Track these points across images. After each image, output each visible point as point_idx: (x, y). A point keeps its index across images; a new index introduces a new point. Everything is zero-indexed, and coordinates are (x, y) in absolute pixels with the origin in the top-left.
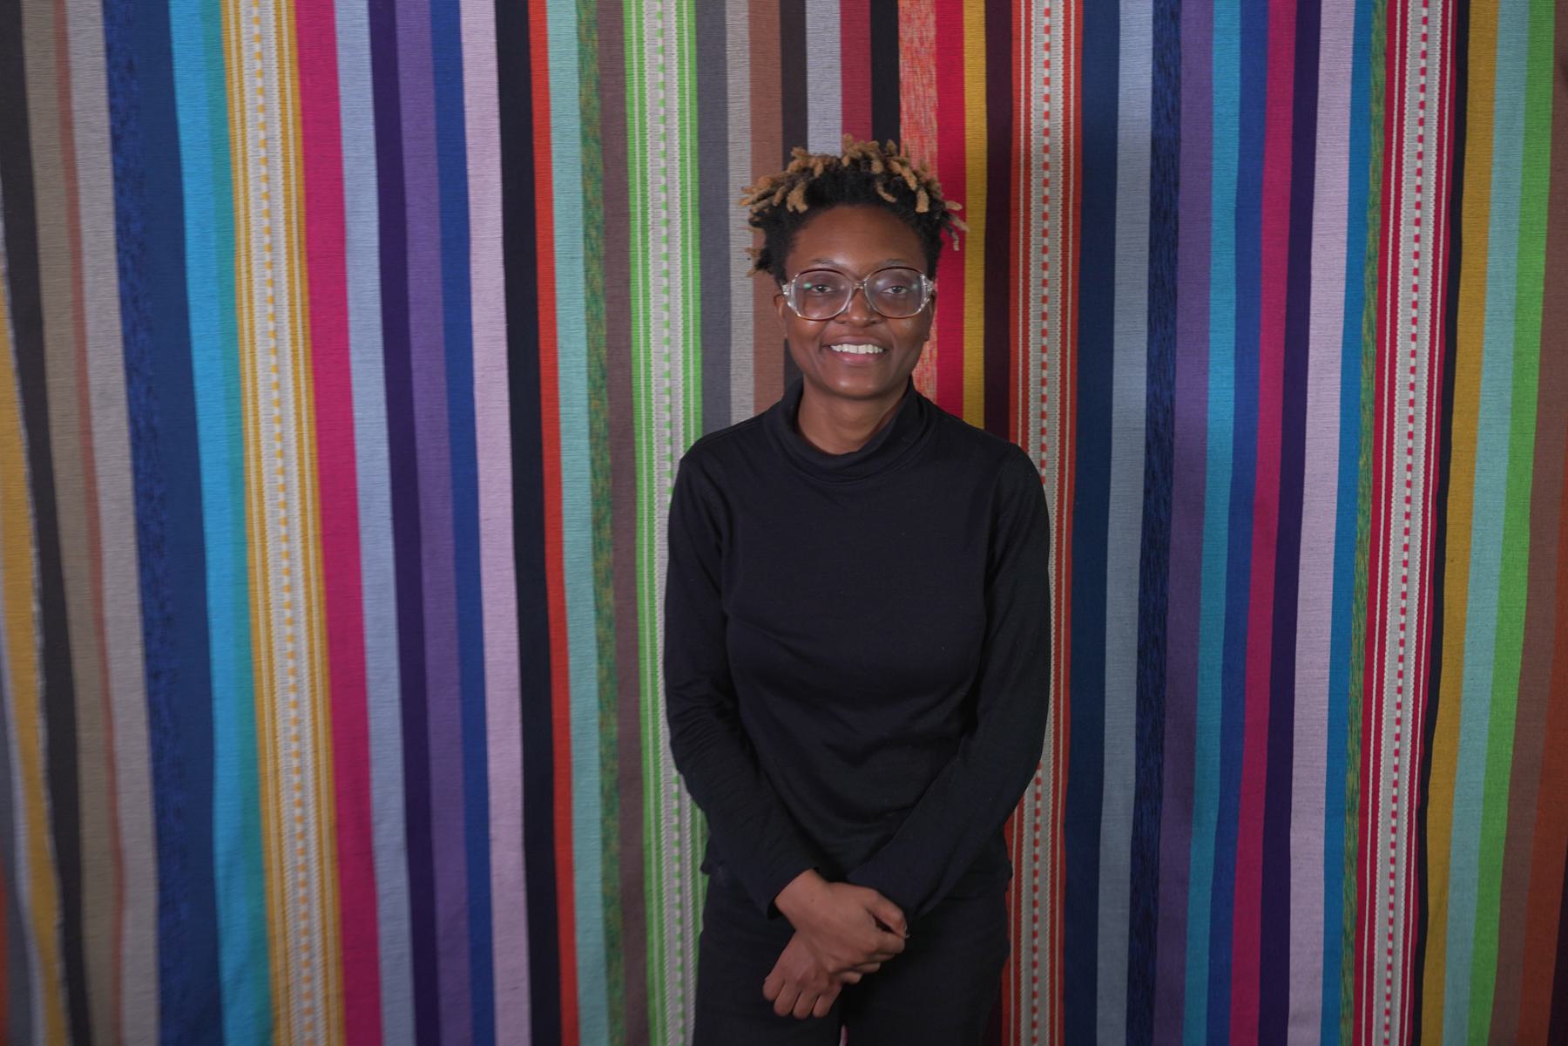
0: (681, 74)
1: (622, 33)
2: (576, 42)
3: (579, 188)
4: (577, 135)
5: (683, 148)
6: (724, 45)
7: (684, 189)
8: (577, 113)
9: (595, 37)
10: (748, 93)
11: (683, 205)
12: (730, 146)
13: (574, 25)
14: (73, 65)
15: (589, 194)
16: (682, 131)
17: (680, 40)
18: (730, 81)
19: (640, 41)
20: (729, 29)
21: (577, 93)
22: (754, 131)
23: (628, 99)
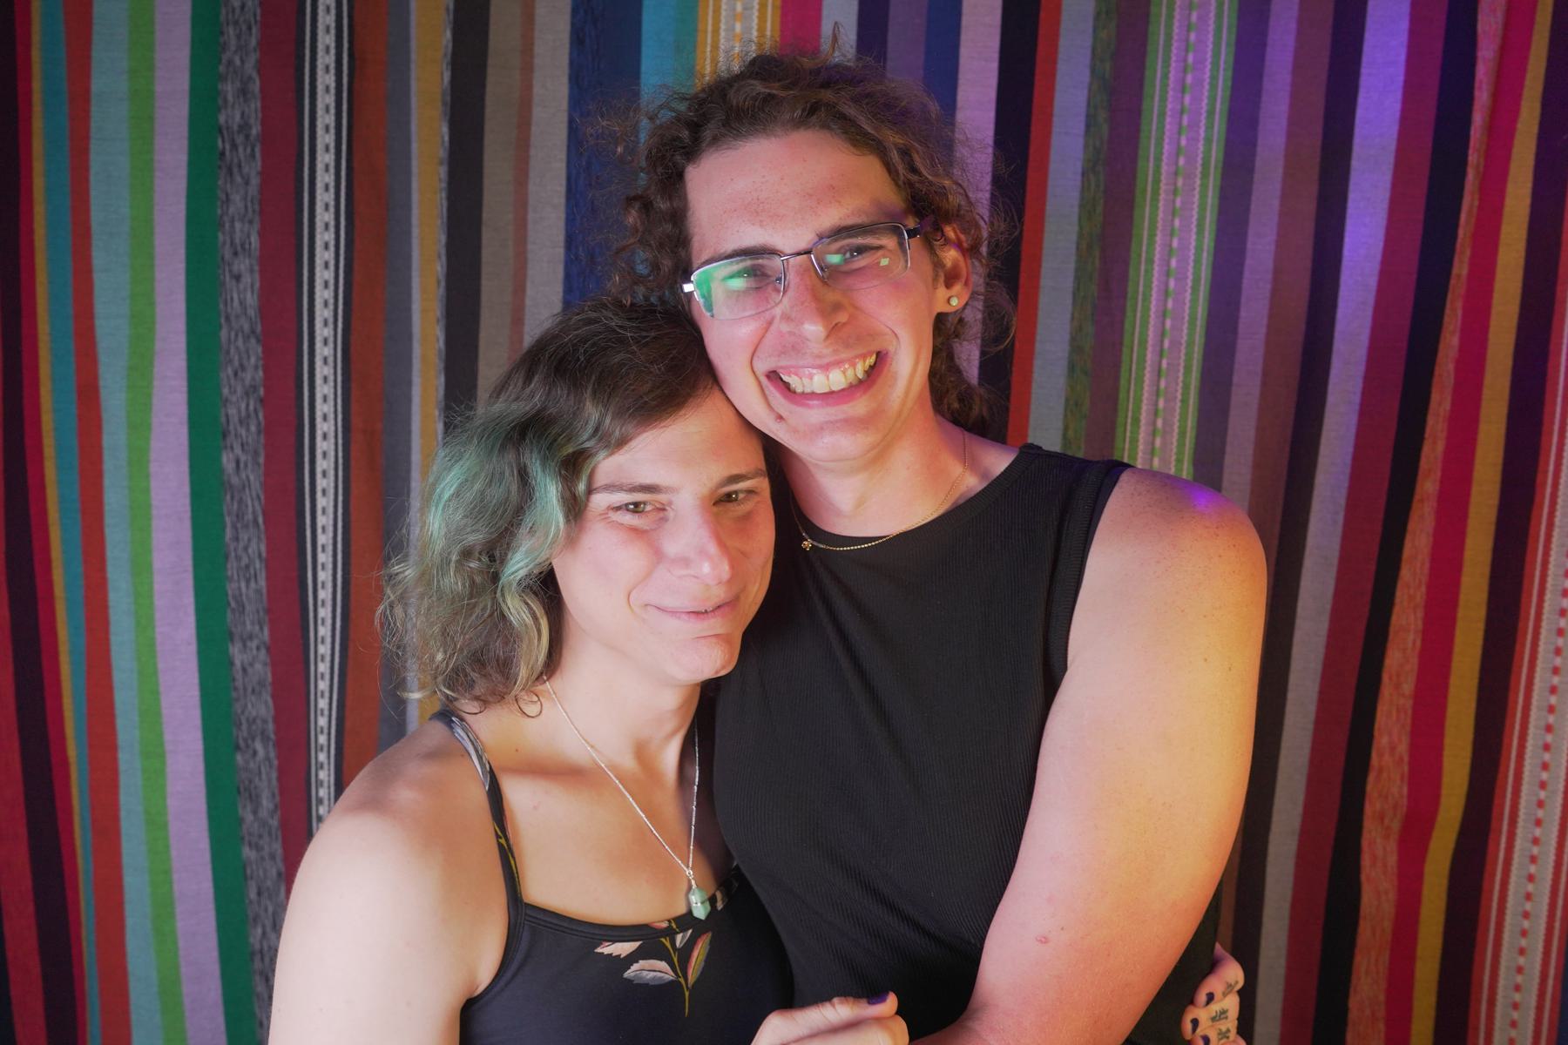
0: (1194, 301)
1: (1128, 250)
2: (1073, 258)
3: (1060, 424)
4: (1065, 363)
5: (1186, 387)
6: (1241, 273)
7: (1182, 434)
8: (1067, 337)
9: (1097, 253)
10: (1264, 330)
11: (1180, 453)
12: (1234, 389)
13: (1074, 237)
14: (530, 256)
15: (1071, 433)
16: (1188, 368)
17: (1197, 261)
18: (1243, 314)
19: (1150, 261)
20: (1249, 254)
21: (1069, 316)
22: (1265, 374)
23: (1127, 326)
